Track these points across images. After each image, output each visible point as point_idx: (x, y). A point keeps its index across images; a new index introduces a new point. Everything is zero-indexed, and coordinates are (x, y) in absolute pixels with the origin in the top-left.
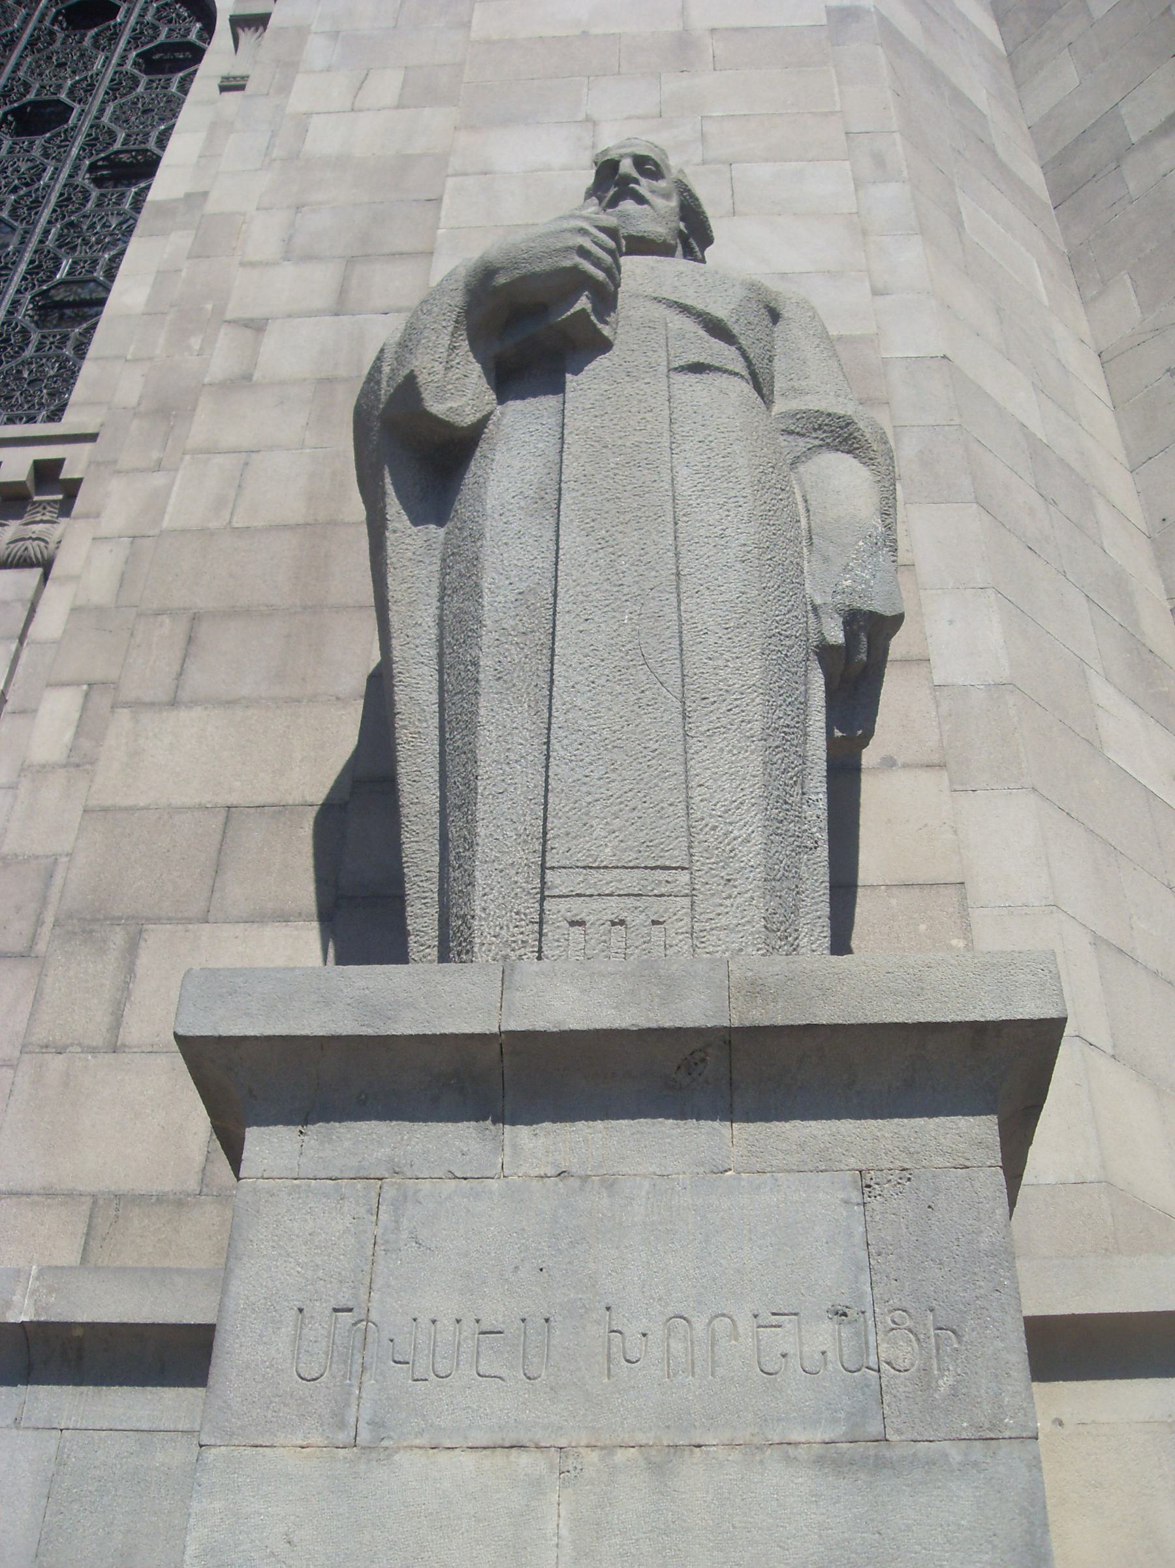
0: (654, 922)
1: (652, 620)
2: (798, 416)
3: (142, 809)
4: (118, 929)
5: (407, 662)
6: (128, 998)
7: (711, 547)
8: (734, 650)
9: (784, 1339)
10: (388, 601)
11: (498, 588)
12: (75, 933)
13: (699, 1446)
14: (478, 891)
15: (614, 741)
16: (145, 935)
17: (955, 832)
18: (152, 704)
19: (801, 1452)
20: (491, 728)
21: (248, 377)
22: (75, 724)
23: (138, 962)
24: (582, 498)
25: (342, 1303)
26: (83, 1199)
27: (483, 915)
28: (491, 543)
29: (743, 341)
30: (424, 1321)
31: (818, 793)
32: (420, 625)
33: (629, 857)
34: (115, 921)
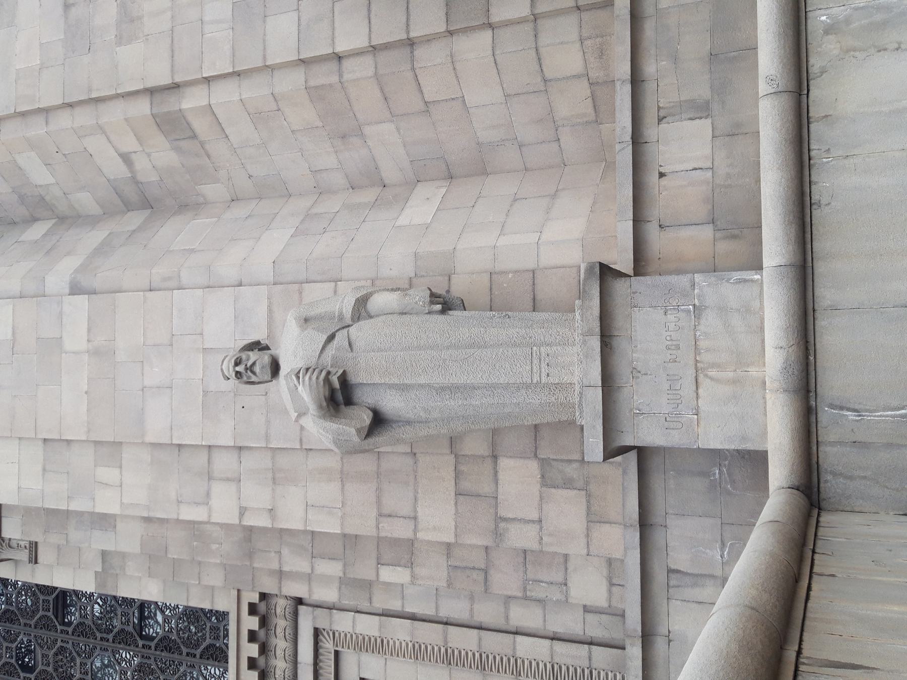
3: (456, 523)
4: (499, 525)
18: (415, 526)
23: (511, 517)
34: (497, 527)
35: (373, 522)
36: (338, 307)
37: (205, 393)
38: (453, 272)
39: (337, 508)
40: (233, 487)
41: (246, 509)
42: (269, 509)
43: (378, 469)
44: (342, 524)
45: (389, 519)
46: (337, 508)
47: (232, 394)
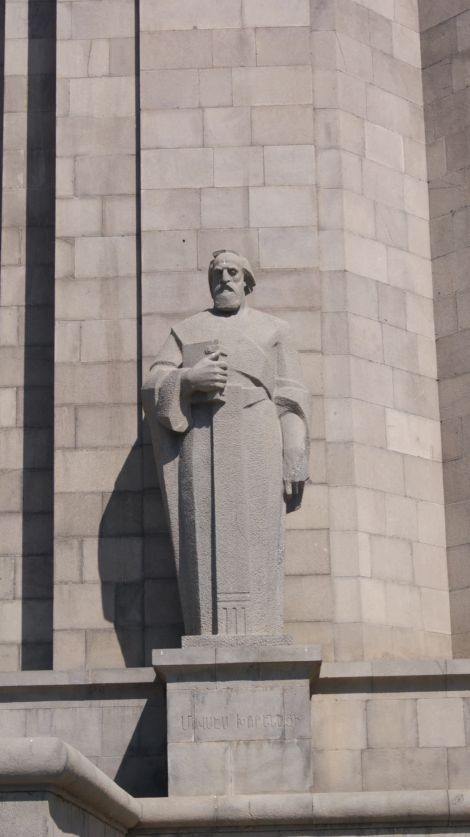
0: (242, 608)
1: (240, 514)
2: (282, 399)
3: (74, 493)
4: (75, 540)
5: (172, 505)
6: (83, 565)
7: (254, 480)
9: (268, 721)
10: (165, 485)
11: (198, 496)
12: (62, 542)
13: (254, 740)
14: (200, 593)
15: (231, 555)
16: (84, 542)
18: (68, 448)
20: (200, 544)
21: (73, 276)
22: (16, 407)
23: (84, 552)
24: (220, 468)
25: (190, 714)
26: (82, 631)
27: (202, 600)
28: (195, 479)
31: (283, 544)
32: (175, 493)
34: (73, 537)
37: (199, 192)
38: (332, 485)
39: (80, 357)
40: (95, 227)
41: (73, 244)
42: (74, 274)
43: (124, 404)
44: (64, 364)
45: (72, 418)
46: (80, 357)
47: (198, 227)
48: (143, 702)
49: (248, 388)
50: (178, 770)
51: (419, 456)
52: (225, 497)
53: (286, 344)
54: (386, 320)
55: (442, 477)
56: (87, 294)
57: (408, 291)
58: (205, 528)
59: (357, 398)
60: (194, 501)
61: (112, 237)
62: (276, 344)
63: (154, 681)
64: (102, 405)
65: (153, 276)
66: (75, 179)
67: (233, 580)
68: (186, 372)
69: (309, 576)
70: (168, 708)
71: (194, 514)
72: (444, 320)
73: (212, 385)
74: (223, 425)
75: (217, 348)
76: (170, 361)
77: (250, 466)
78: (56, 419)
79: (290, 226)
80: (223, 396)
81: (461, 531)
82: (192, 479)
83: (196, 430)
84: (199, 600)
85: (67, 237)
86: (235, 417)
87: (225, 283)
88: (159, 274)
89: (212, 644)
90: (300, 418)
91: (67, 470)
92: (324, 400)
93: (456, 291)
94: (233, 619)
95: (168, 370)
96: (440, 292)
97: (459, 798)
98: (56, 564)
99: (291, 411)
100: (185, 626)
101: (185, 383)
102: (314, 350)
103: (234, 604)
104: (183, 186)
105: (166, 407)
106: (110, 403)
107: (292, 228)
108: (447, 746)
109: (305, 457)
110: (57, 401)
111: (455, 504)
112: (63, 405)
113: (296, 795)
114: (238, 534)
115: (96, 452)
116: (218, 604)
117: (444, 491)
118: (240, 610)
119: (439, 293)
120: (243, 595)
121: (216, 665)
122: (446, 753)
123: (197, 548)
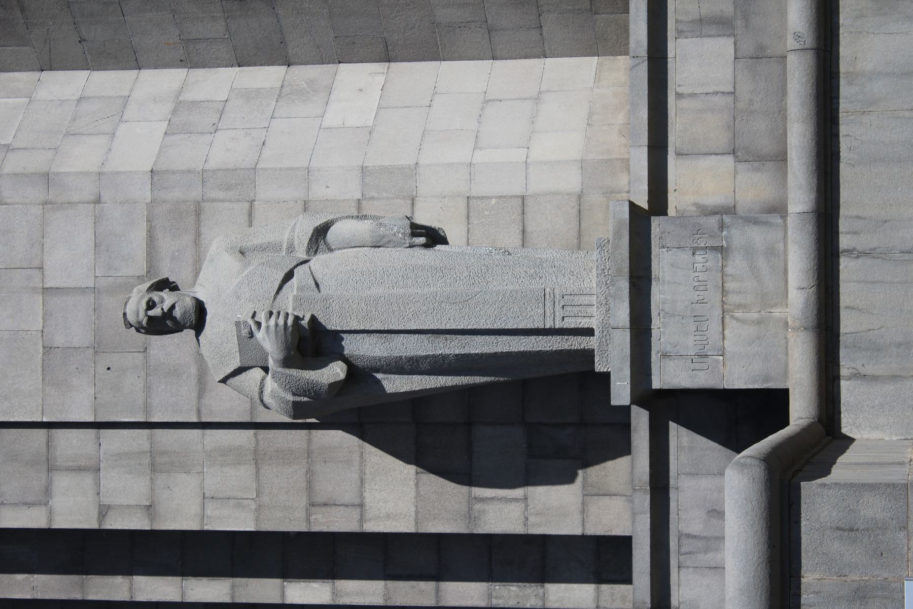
0: (563, 298)
2: (310, 247)
3: (417, 508)
4: (474, 507)
6: (505, 498)
8: (452, 274)
9: (699, 266)
11: (426, 349)
16: (477, 496)
17: (445, 197)
18: (361, 515)
19: (724, 264)
21: (149, 507)
24: (393, 322)
29: (291, 267)
30: (695, 343)
33: (541, 305)
34: (470, 509)
35: (300, 514)
36: (286, 237)
38: (415, 193)
40: (88, 480)
41: (109, 507)
42: (146, 506)
43: (309, 446)
44: (257, 519)
45: (324, 509)
47: (91, 351)
48: (673, 426)
49: (296, 286)
50: (757, 376)
51: (381, 90)
52: (428, 317)
53: (241, 241)
54: (214, 125)
55: (407, 63)
56: (171, 490)
57: (178, 98)
58: (465, 342)
59: (309, 160)
60: (432, 355)
61: (101, 459)
62: (242, 253)
63: (648, 410)
64: (310, 475)
65: (151, 407)
66: (26, 504)
67: (529, 308)
68: (275, 361)
69: (525, 221)
70: (681, 388)
71: (448, 356)
72: (214, 56)
73: (290, 329)
74: (339, 317)
75: (245, 323)
76: (259, 384)
77: (391, 285)
78: (325, 529)
79: (94, 237)
80: (304, 316)
81: (474, 41)
82: (405, 356)
83: (346, 352)
84: (552, 350)
85: (99, 514)
86: (330, 303)
87: (164, 313)
88: (149, 400)
89: (606, 335)
90: (334, 226)
91: (388, 516)
92: (311, 201)
93: (180, 39)
94: (577, 309)
95: (270, 384)
96: (180, 60)
97: (798, 36)
98: (502, 531)
99: (325, 237)
100: (582, 370)
101: (287, 362)
102: (249, 211)
103: (558, 308)
104: (40, 369)
105: (316, 386)
106: (308, 463)
107: (97, 234)
108: (733, 58)
109: (381, 220)
110: (302, 528)
111: (440, 48)
112: (308, 520)
113: (789, 233)
114: (474, 301)
115: (367, 481)
116: (557, 327)
117: (425, 61)
118: (566, 301)
119: (181, 61)
120: (547, 296)
121: (631, 328)
122: (742, 60)
123: (488, 351)
